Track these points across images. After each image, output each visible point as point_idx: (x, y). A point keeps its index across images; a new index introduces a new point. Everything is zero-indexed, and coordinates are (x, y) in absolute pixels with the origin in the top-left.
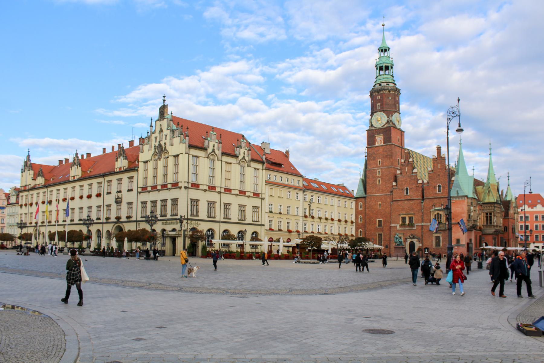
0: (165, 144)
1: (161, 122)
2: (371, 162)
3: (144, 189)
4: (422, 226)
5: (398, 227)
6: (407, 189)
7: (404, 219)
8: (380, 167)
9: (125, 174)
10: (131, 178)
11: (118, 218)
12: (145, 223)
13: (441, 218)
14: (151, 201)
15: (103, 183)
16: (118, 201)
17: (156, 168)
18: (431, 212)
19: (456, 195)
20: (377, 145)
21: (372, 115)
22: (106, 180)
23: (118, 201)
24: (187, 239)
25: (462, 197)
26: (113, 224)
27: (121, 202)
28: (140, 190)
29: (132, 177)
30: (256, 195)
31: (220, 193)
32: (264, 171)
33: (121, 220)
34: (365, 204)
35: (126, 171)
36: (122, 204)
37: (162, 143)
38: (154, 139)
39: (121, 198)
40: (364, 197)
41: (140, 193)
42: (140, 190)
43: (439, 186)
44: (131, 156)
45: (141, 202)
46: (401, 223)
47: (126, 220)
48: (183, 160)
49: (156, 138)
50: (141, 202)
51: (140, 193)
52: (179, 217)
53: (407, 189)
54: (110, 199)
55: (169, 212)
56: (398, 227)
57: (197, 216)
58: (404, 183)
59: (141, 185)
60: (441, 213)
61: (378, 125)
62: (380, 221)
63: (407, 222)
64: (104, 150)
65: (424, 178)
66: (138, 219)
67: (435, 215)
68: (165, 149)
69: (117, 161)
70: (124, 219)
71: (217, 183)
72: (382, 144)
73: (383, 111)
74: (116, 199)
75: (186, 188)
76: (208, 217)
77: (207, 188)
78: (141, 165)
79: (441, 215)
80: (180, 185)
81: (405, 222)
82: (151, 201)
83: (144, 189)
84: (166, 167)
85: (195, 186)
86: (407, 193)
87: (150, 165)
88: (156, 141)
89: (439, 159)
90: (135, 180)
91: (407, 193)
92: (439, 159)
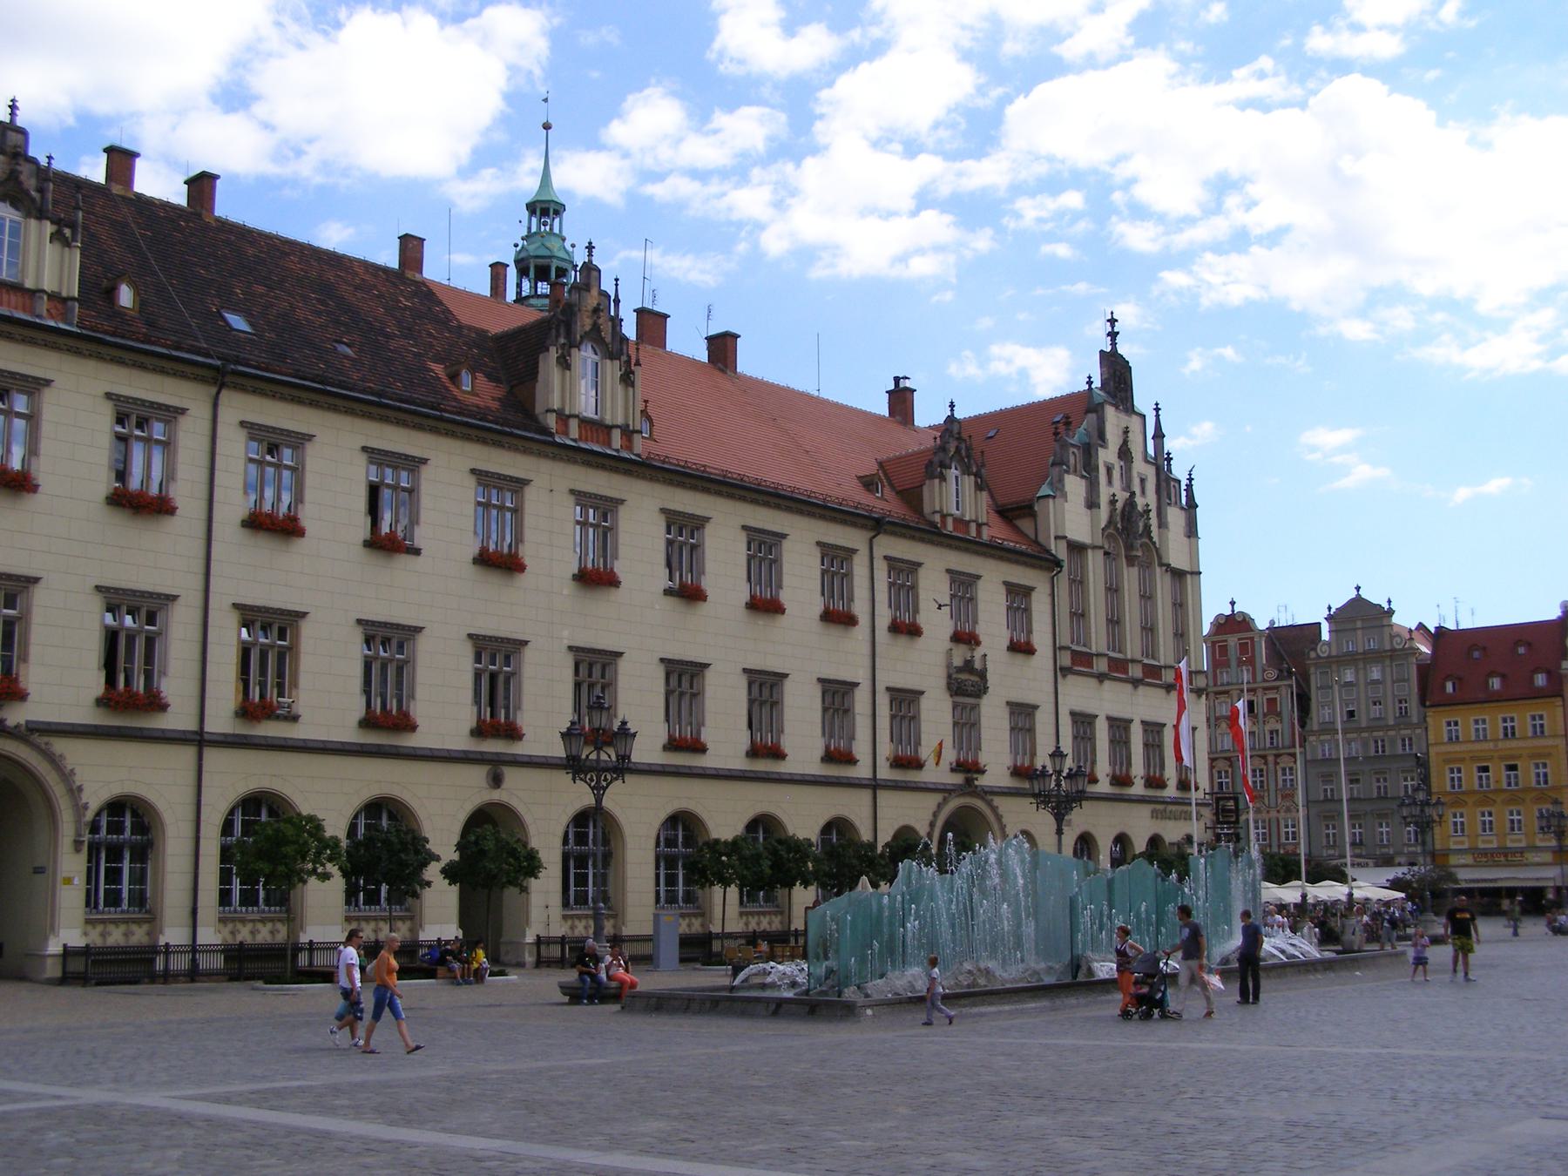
11: (969, 768)
12: (1027, 805)
14: (1109, 718)
16: (967, 684)
22: (879, 552)
23: (967, 684)
26: (938, 797)
27: (981, 690)
33: (983, 781)
39: (982, 674)
42: (1065, 659)
45: (1073, 714)
47: (1006, 781)
50: (1073, 714)
55: (1138, 769)
69: (943, 478)
70: (996, 772)
82: (1109, 718)
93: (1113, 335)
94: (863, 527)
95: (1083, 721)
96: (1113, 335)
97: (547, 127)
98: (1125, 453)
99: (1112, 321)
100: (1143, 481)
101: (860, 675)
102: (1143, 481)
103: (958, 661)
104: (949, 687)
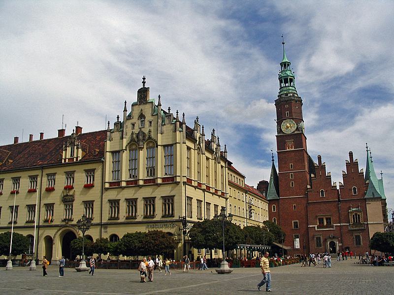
0: (150, 131)
1: (142, 107)
2: (284, 165)
3: (116, 185)
4: (340, 226)
5: (316, 228)
6: (322, 191)
7: (321, 221)
8: (292, 170)
9: (81, 166)
10: (90, 173)
13: (359, 218)
15: (39, 179)
16: (68, 201)
17: (134, 160)
18: (349, 212)
19: (372, 197)
20: (288, 150)
21: (279, 123)
22: (44, 174)
23: (68, 201)
24: (187, 244)
25: (377, 198)
26: (58, 228)
28: (107, 185)
29: (93, 170)
30: (223, 195)
31: (204, 191)
32: (227, 169)
34: (278, 206)
35: (82, 162)
36: (75, 204)
37: (146, 132)
38: (130, 126)
39: (73, 196)
40: (278, 199)
41: (107, 189)
42: (107, 185)
43: (355, 189)
44: (93, 145)
46: (318, 224)
48: (181, 150)
49: (133, 125)
51: (107, 189)
52: (176, 218)
53: (322, 191)
54: (55, 198)
56: (316, 228)
57: (191, 218)
58: (319, 186)
59: (108, 178)
60: (358, 214)
61: (289, 132)
62: (296, 223)
63: (325, 223)
64: (16, 139)
65: (337, 180)
66: (103, 221)
67: (354, 216)
68: (150, 138)
71: (204, 181)
72: (293, 149)
73: (293, 119)
74: (64, 196)
75: (185, 183)
76: (198, 219)
77: (196, 184)
78: (108, 156)
79: (359, 215)
80: (178, 179)
81: (323, 223)
82: (126, 199)
83: (116, 185)
84: (152, 158)
85: (189, 182)
86: (323, 195)
87: (125, 156)
88: (133, 128)
89: (352, 165)
90: (98, 174)
91: (323, 195)
92: (352, 165)
93: (144, 83)
94: (39, 169)
95: (114, 203)
96: (144, 83)
97: (283, 43)
98: (142, 116)
99: (144, 79)
100: (151, 122)
101: (37, 203)
102: (151, 122)
103: (65, 194)
104: (62, 201)
